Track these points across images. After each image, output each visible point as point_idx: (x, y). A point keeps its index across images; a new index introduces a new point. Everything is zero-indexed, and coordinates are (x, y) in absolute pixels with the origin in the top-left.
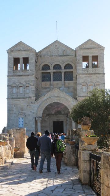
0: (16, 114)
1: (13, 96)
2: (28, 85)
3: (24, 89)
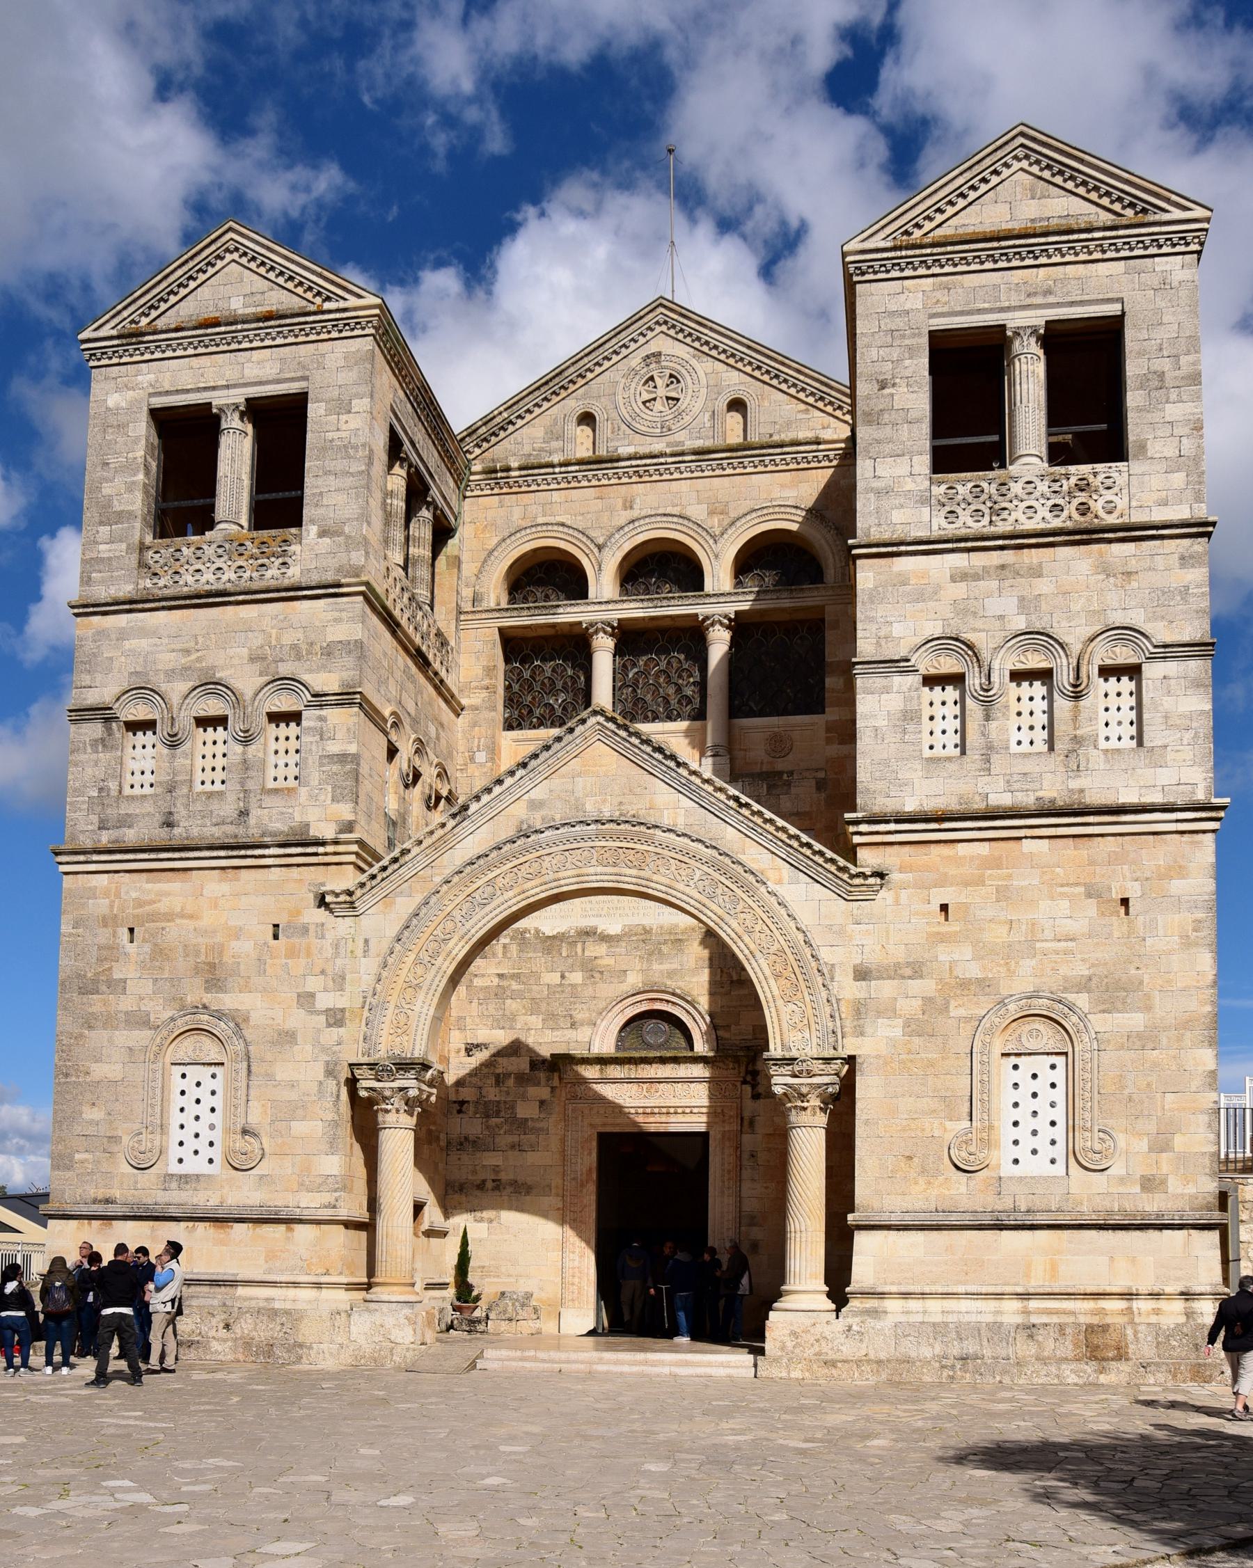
0: (144, 1021)
1: (125, 821)
2: (285, 703)
3: (246, 740)
